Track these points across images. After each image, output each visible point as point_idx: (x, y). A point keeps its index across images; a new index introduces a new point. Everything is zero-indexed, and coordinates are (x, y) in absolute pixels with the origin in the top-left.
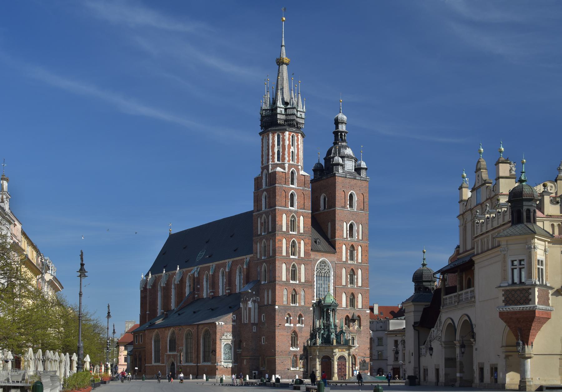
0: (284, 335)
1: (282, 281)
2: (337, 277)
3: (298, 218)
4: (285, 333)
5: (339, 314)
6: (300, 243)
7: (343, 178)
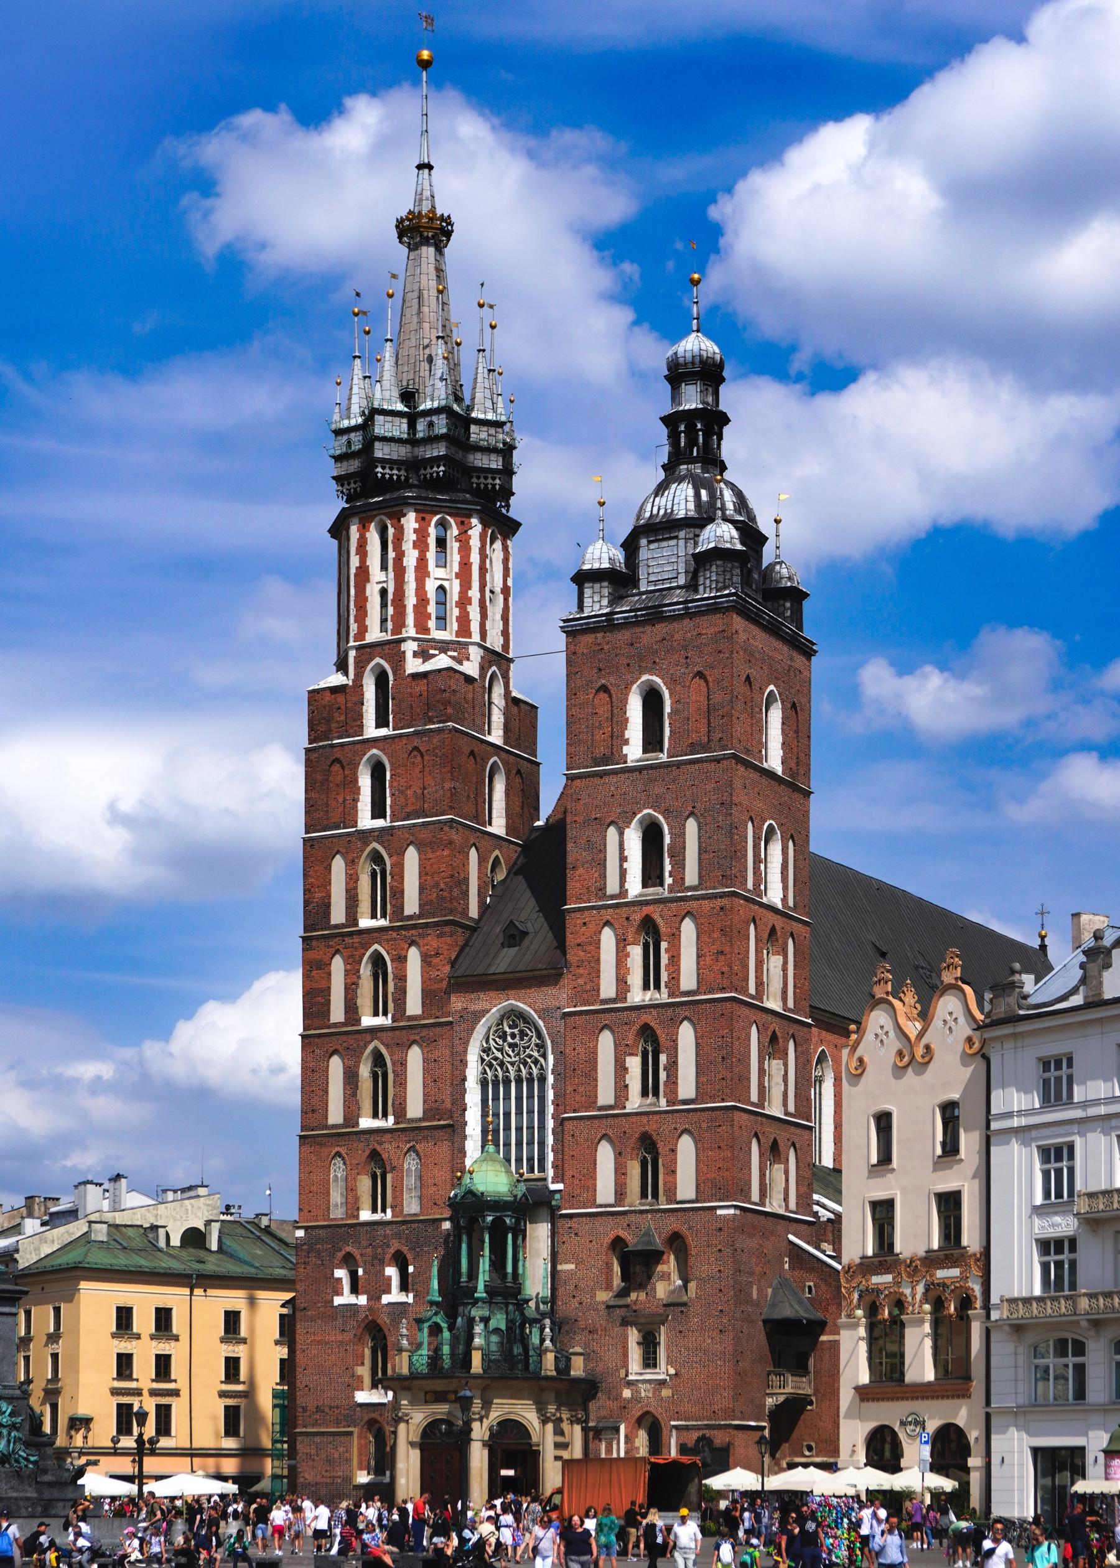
0: (327, 1343)
1: (327, 1127)
2: (570, 1073)
3: (395, 858)
4: (335, 1336)
5: (576, 1234)
6: (401, 960)
7: (600, 635)
